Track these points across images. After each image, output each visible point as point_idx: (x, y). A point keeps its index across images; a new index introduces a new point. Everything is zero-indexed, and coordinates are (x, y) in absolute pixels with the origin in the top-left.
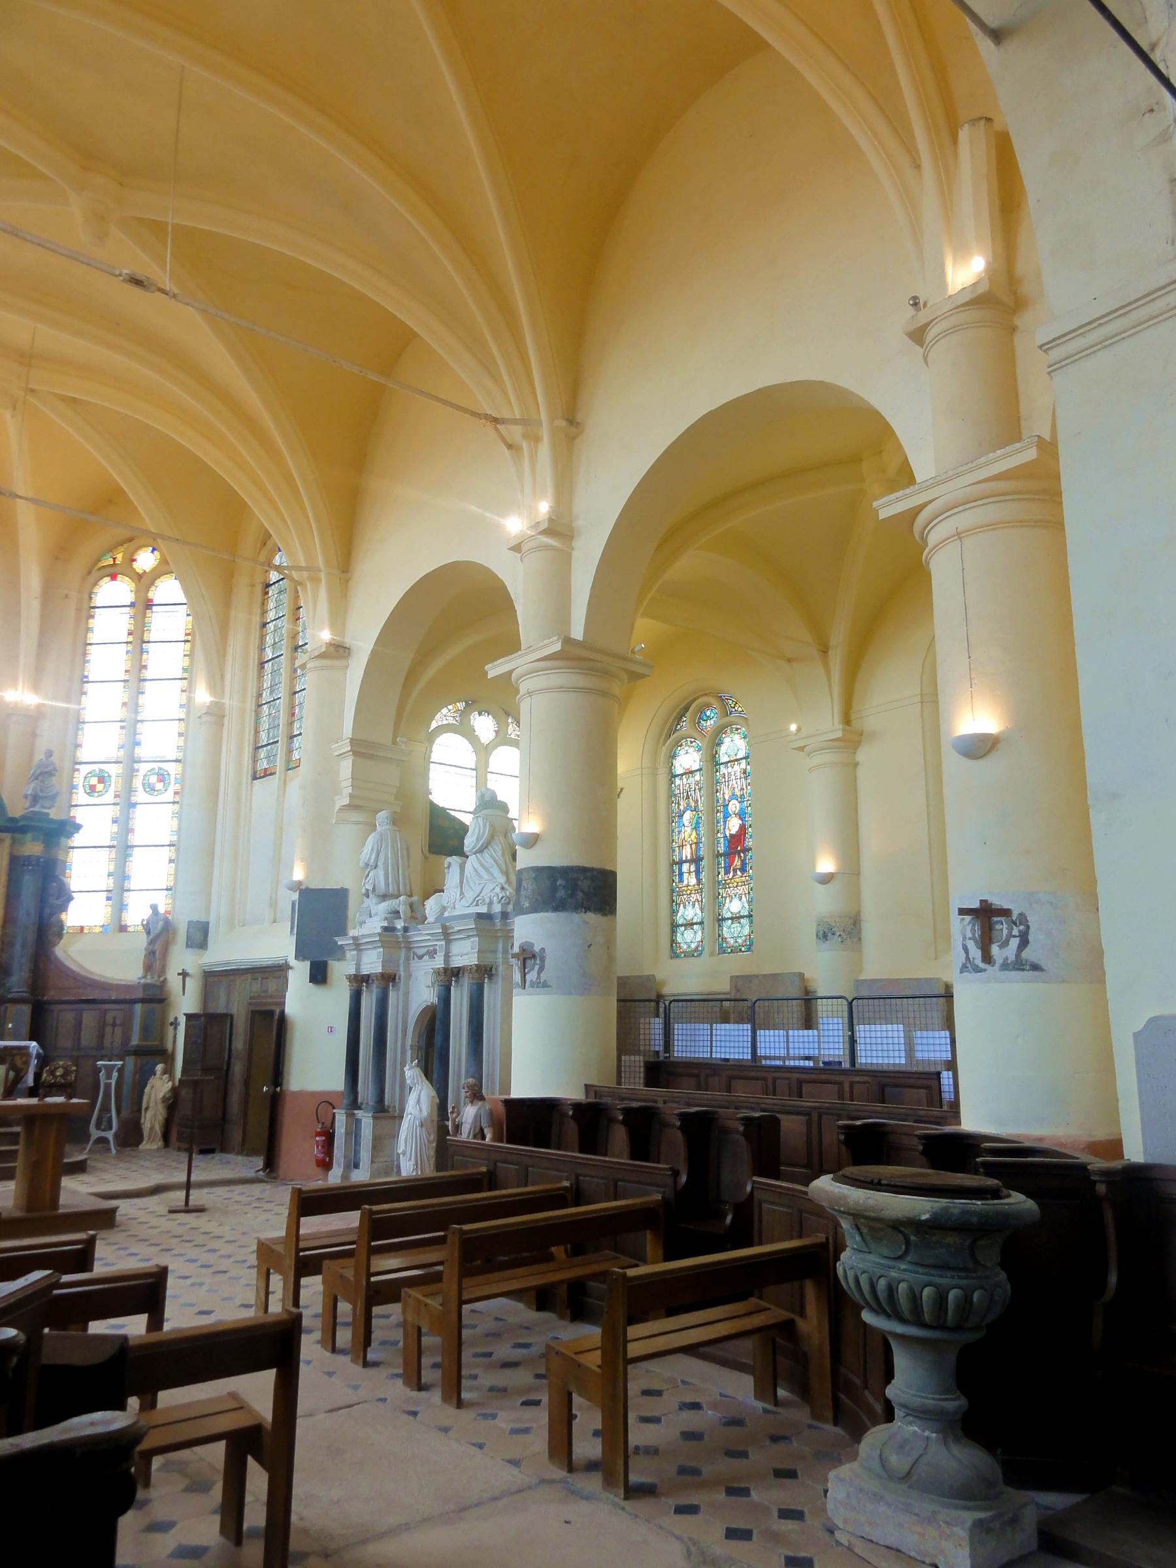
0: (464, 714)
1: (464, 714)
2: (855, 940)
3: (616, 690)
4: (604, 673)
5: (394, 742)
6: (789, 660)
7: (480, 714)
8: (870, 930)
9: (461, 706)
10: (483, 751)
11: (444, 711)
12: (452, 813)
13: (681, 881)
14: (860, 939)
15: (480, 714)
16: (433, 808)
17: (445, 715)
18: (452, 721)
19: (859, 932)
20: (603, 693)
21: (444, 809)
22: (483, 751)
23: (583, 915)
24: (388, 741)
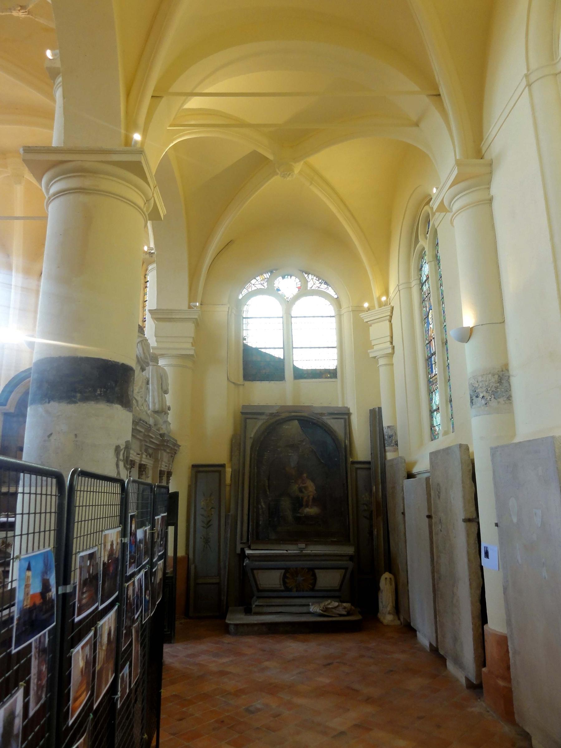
0: (270, 282)
1: (270, 282)
2: (501, 400)
3: (106, 184)
4: (81, 171)
5: (190, 307)
6: (417, 125)
7: (283, 278)
8: (518, 384)
9: (267, 276)
10: (288, 304)
11: (253, 281)
12: (263, 350)
13: (432, 372)
14: (509, 398)
15: (283, 278)
16: (247, 350)
17: (257, 283)
18: (259, 286)
19: (508, 389)
20: (81, 190)
21: (256, 349)
22: (288, 304)
23: (47, 405)
24: (185, 307)
